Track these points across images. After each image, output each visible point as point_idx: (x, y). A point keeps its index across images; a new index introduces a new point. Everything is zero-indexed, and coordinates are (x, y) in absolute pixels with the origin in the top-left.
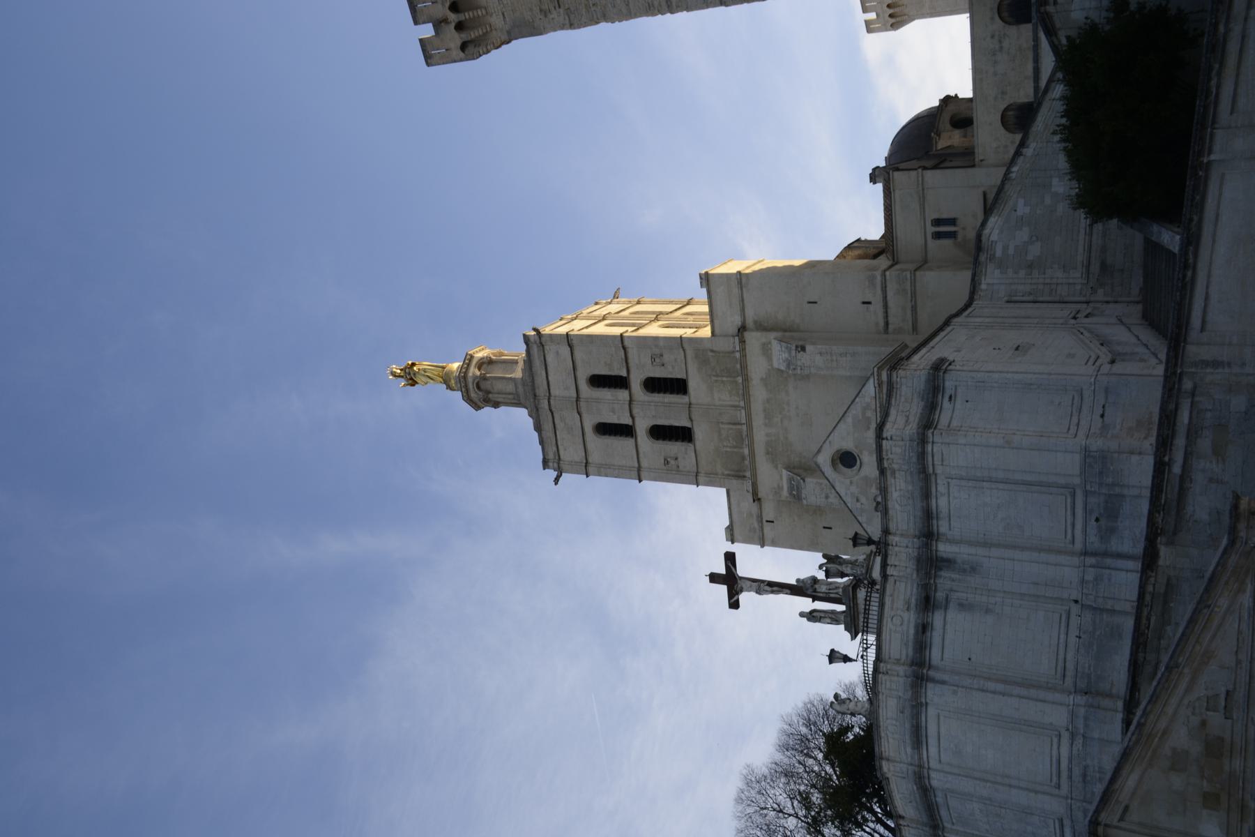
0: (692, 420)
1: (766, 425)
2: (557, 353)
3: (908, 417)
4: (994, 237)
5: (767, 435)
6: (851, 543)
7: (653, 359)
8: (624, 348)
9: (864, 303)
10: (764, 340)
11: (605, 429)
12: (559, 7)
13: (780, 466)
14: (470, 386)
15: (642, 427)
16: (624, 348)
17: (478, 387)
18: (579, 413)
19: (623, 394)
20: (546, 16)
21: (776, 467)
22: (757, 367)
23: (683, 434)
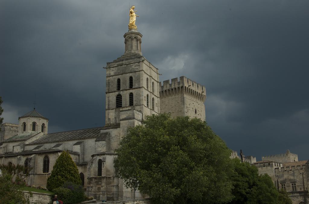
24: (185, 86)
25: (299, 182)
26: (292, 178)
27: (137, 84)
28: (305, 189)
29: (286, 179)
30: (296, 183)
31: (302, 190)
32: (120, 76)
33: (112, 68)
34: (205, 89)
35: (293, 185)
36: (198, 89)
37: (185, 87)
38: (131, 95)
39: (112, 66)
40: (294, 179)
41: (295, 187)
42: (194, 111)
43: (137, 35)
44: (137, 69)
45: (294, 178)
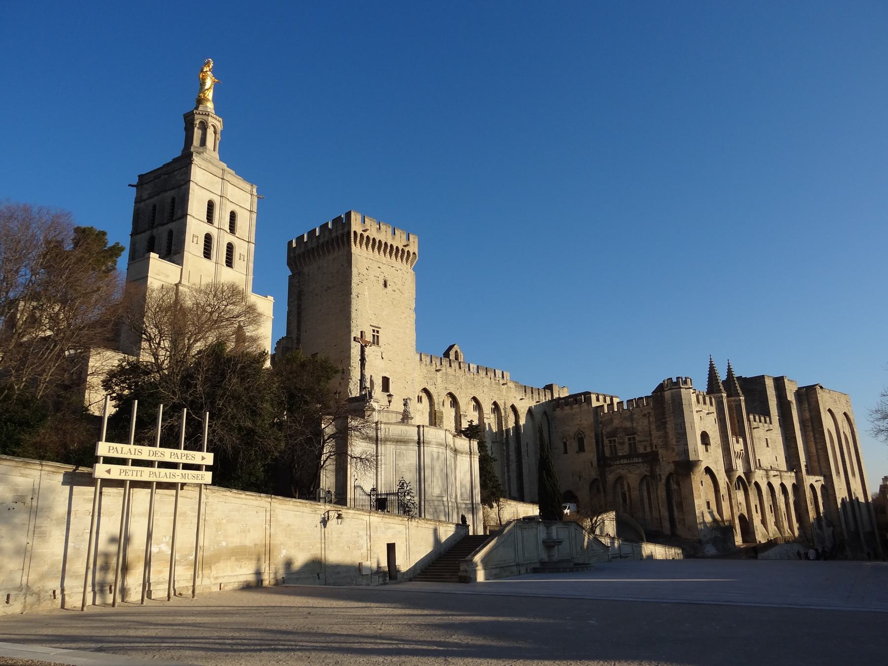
24: (353, 230)
25: (641, 432)
26: (628, 424)
27: (180, 211)
28: (654, 449)
29: (617, 428)
30: (636, 436)
31: (649, 450)
32: (156, 198)
33: (145, 186)
34: (416, 241)
35: (629, 439)
36: (393, 239)
37: (355, 233)
38: (171, 233)
39: (146, 181)
40: (633, 427)
41: (635, 443)
42: (382, 282)
43: (205, 117)
44: (183, 180)
45: (632, 424)
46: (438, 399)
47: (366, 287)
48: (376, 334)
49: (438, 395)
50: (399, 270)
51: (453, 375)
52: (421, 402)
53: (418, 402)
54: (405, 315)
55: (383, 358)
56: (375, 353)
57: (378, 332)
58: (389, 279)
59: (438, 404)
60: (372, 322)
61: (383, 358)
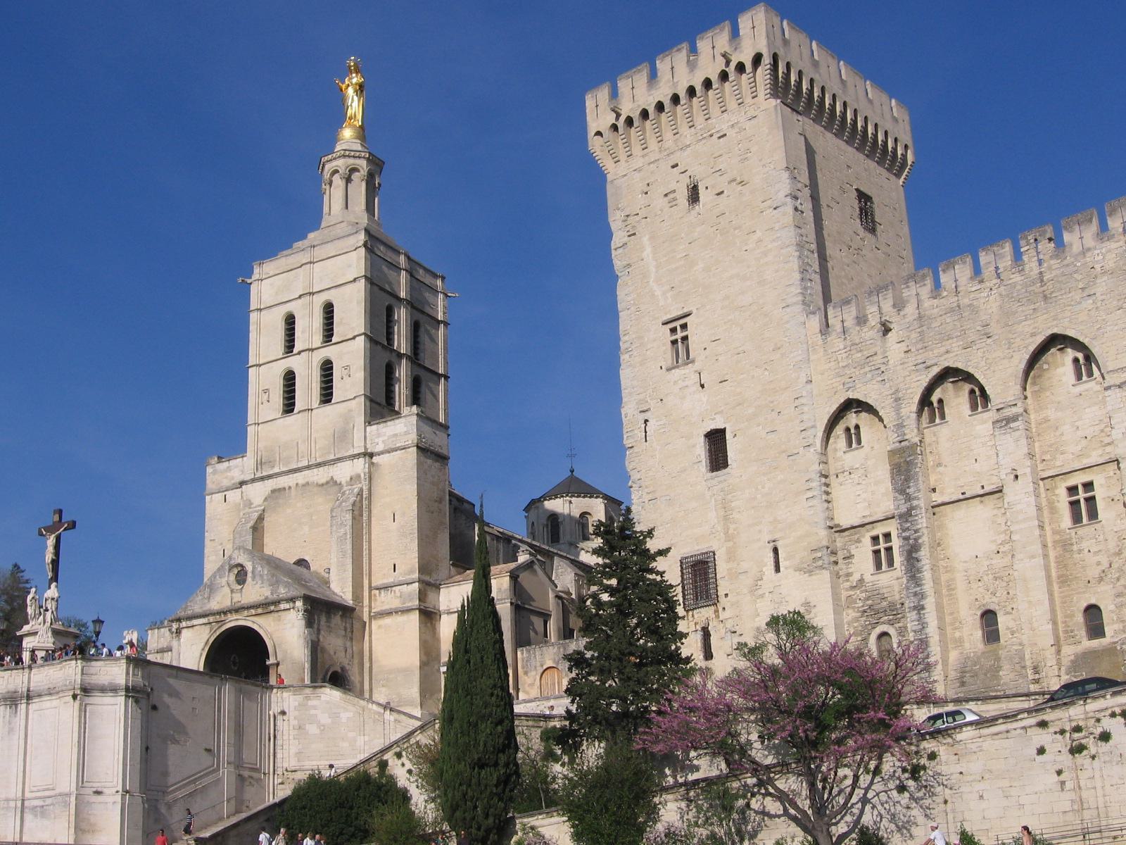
0: (299, 412)
1: (297, 484)
2: (350, 266)
3: (96, 674)
4: (323, 697)
5: (290, 488)
6: (95, 618)
7: (347, 367)
8: (354, 338)
9: (395, 565)
10: (362, 475)
11: (290, 321)
12: (629, 236)
13: (265, 503)
14: (335, 163)
15: (294, 363)
16: (354, 338)
17: (336, 172)
18: (300, 297)
19: (318, 339)
20: (624, 221)
21: (266, 499)
22: (342, 472)
23: (289, 407)
46: (898, 410)
47: (645, 239)
48: (680, 334)
49: (897, 400)
50: (731, 133)
51: (952, 310)
52: (859, 442)
53: (850, 444)
54: (759, 234)
55: (702, 386)
56: (681, 384)
57: (684, 327)
58: (698, 171)
59: (900, 426)
60: (666, 314)
61: (702, 386)
